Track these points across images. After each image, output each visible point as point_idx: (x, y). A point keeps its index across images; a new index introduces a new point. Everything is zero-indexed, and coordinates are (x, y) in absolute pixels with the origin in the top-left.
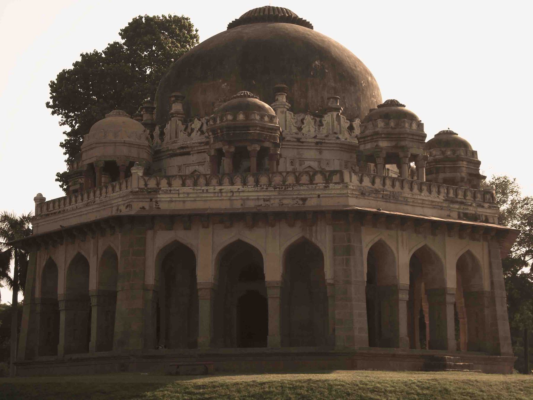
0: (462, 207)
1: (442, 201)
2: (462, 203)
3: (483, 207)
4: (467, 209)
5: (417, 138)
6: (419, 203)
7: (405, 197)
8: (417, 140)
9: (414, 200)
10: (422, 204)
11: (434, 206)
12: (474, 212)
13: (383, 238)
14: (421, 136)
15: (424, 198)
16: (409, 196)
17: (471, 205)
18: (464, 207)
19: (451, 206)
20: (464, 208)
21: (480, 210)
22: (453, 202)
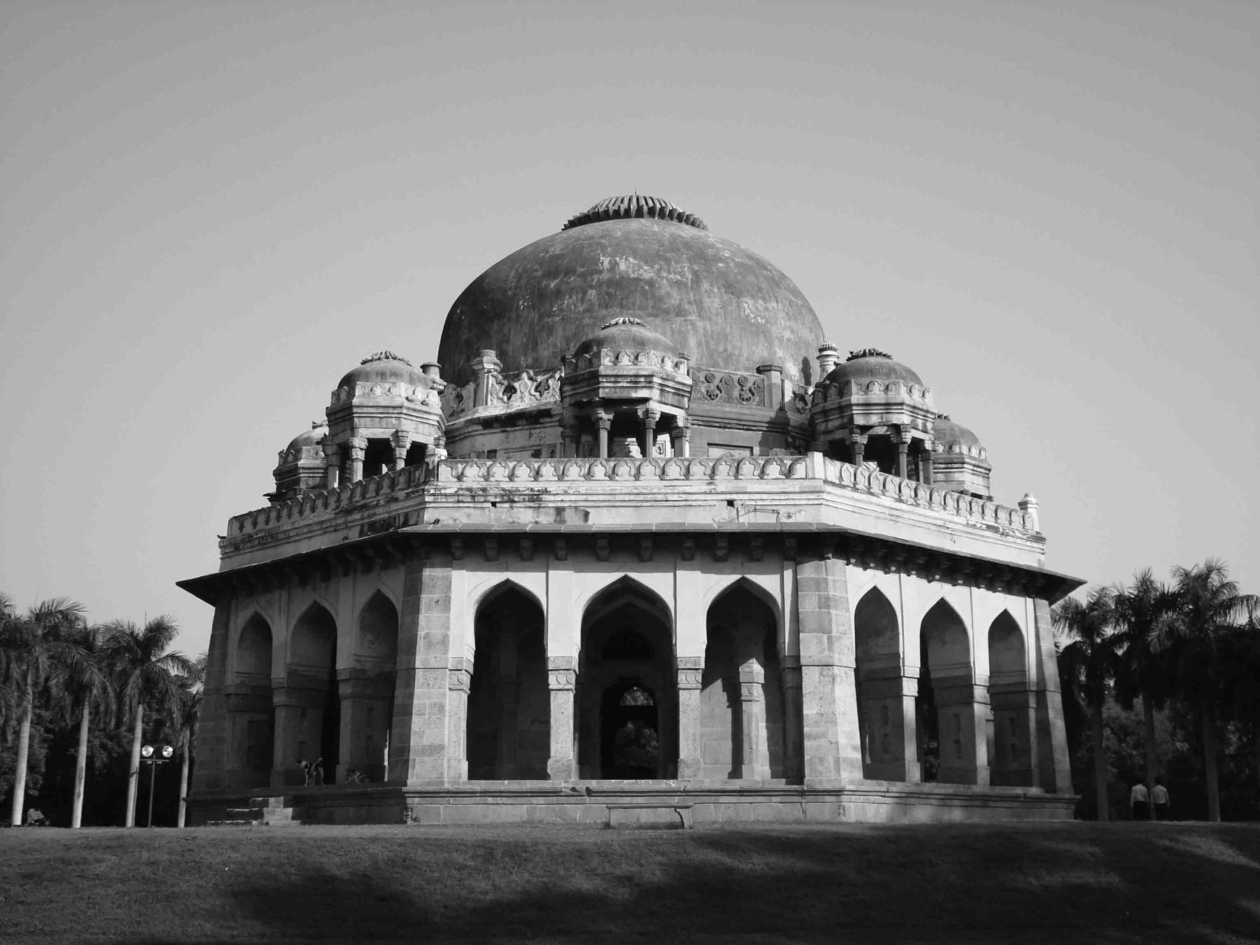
0: (366, 514)
1: (333, 516)
2: (364, 507)
3: (396, 500)
4: (375, 514)
5: (342, 414)
6: (306, 533)
7: (285, 532)
8: (342, 418)
9: (296, 531)
10: (310, 532)
11: (324, 528)
12: (386, 515)
13: (259, 610)
14: (346, 409)
15: (310, 522)
16: (289, 528)
17: (377, 506)
18: (367, 512)
19: (350, 518)
20: (368, 516)
21: (394, 506)
22: (349, 512)
